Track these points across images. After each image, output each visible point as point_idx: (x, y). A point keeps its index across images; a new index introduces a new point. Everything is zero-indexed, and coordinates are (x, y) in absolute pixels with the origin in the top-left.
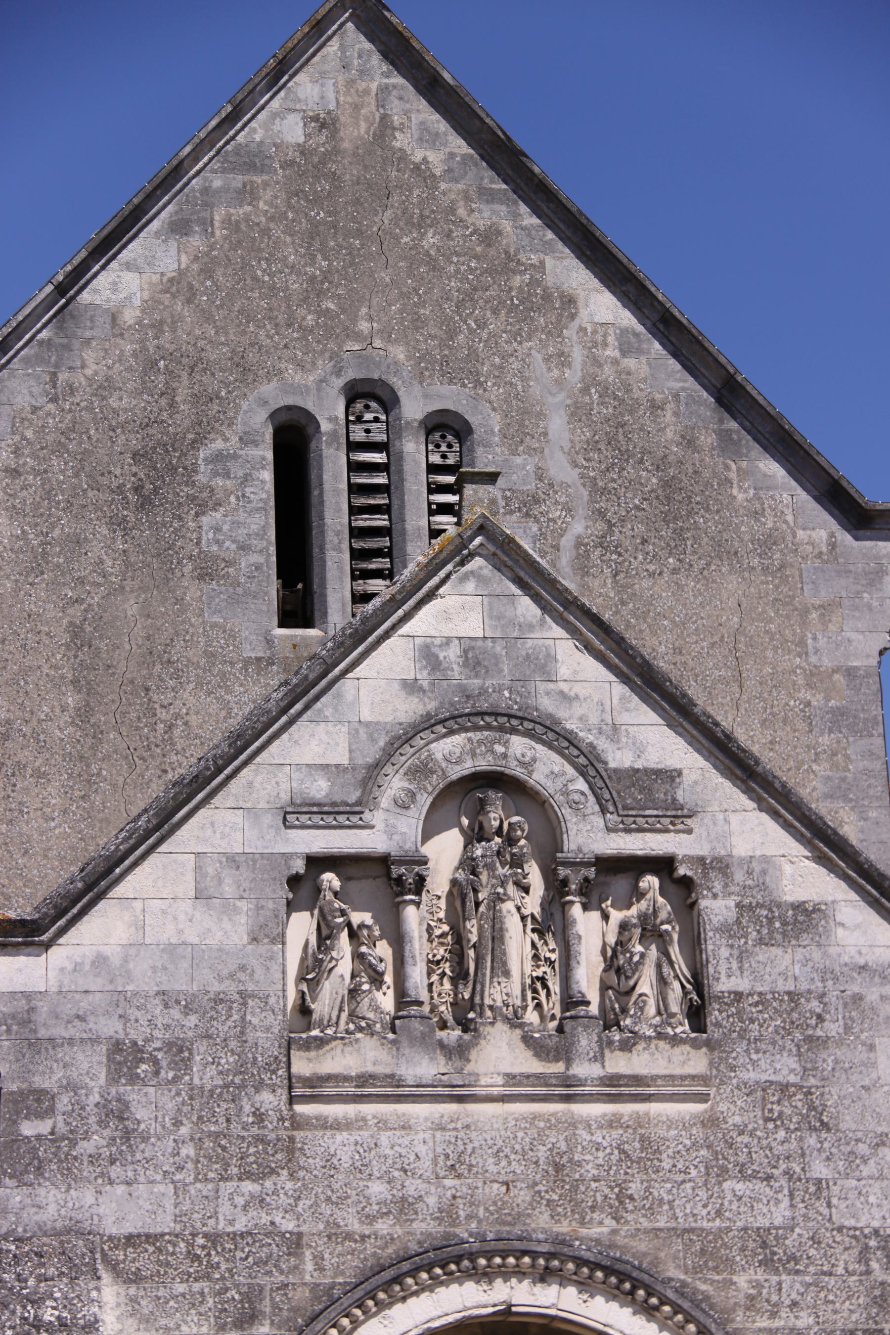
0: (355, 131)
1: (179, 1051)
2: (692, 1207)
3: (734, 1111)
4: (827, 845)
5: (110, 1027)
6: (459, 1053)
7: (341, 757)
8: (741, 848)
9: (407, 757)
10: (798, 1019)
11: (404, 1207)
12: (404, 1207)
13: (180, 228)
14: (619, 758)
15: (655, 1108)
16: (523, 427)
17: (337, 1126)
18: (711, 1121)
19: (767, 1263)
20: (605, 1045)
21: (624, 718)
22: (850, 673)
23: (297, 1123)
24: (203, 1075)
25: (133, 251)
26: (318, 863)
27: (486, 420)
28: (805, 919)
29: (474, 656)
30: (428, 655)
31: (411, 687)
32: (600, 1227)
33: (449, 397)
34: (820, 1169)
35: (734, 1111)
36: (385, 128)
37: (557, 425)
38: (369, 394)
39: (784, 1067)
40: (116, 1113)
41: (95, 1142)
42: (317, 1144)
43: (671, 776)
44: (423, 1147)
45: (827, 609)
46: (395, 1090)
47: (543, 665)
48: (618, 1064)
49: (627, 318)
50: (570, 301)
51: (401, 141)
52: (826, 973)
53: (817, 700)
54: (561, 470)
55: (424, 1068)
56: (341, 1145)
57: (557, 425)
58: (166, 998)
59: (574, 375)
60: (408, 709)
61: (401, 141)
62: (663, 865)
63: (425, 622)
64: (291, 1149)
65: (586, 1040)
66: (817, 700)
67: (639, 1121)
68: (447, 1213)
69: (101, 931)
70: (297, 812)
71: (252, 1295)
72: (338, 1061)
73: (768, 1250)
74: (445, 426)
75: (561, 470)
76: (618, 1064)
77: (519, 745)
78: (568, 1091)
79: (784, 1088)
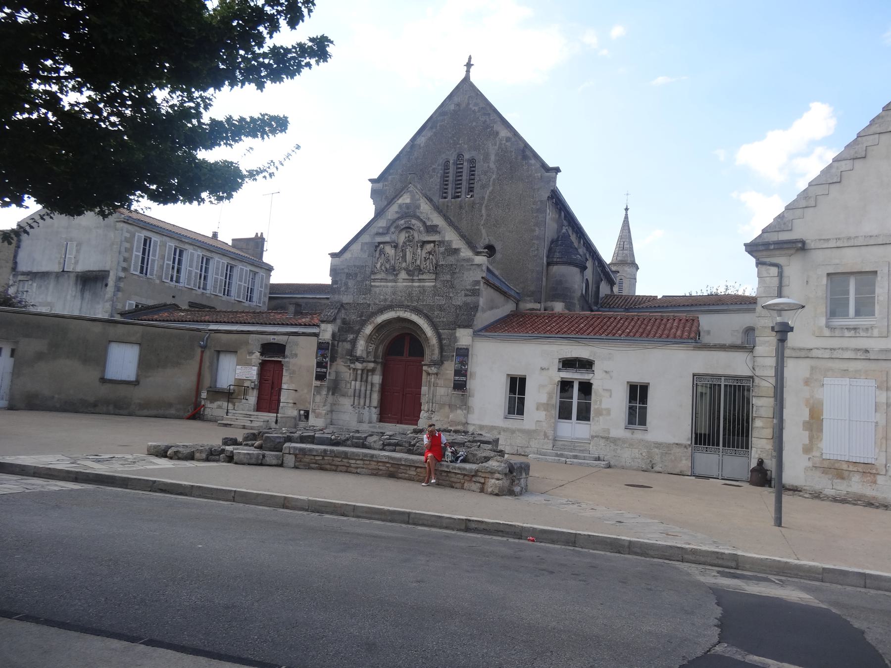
0: (463, 106)
1: (356, 274)
2: (429, 301)
3: (439, 285)
4: (463, 236)
5: (346, 271)
6: (397, 275)
7: (384, 225)
8: (447, 239)
9: (395, 225)
10: (452, 270)
11: (385, 300)
12: (385, 300)
13: (431, 128)
14: (429, 223)
15: (427, 284)
16: (486, 158)
17: (378, 287)
18: (435, 286)
19: (440, 310)
20: (419, 274)
21: (430, 216)
22: (541, 201)
23: (372, 286)
24: (359, 279)
25: (424, 133)
26: (380, 243)
27: (480, 158)
28: (456, 251)
29: (408, 206)
30: (400, 206)
31: (397, 212)
32: (415, 304)
33: (474, 154)
34: (451, 295)
35: (439, 285)
36: (469, 104)
37: (493, 158)
38: (460, 156)
39: (448, 277)
40: (346, 284)
41: (343, 289)
42: (374, 289)
43: (437, 226)
44: (389, 290)
45: (538, 189)
46: (386, 280)
47: (418, 207)
48: (421, 277)
49: (509, 135)
50: (497, 133)
51: (471, 106)
52: (458, 261)
53: (534, 207)
54: (492, 165)
55: (391, 278)
56: (377, 290)
57: (493, 158)
58: (355, 266)
59: (497, 147)
60: (396, 216)
61: (471, 106)
62: (434, 242)
63: (400, 201)
64: (370, 290)
65: (416, 273)
66: (534, 207)
67: (424, 286)
68: (392, 301)
69: (347, 255)
70: (378, 234)
71: (362, 313)
72: (378, 276)
73: (441, 308)
74: (472, 161)
75: (492, 165)
76: (421, 277)
77: (414, 221)
78: (413, 281)
79: (448, 281)
